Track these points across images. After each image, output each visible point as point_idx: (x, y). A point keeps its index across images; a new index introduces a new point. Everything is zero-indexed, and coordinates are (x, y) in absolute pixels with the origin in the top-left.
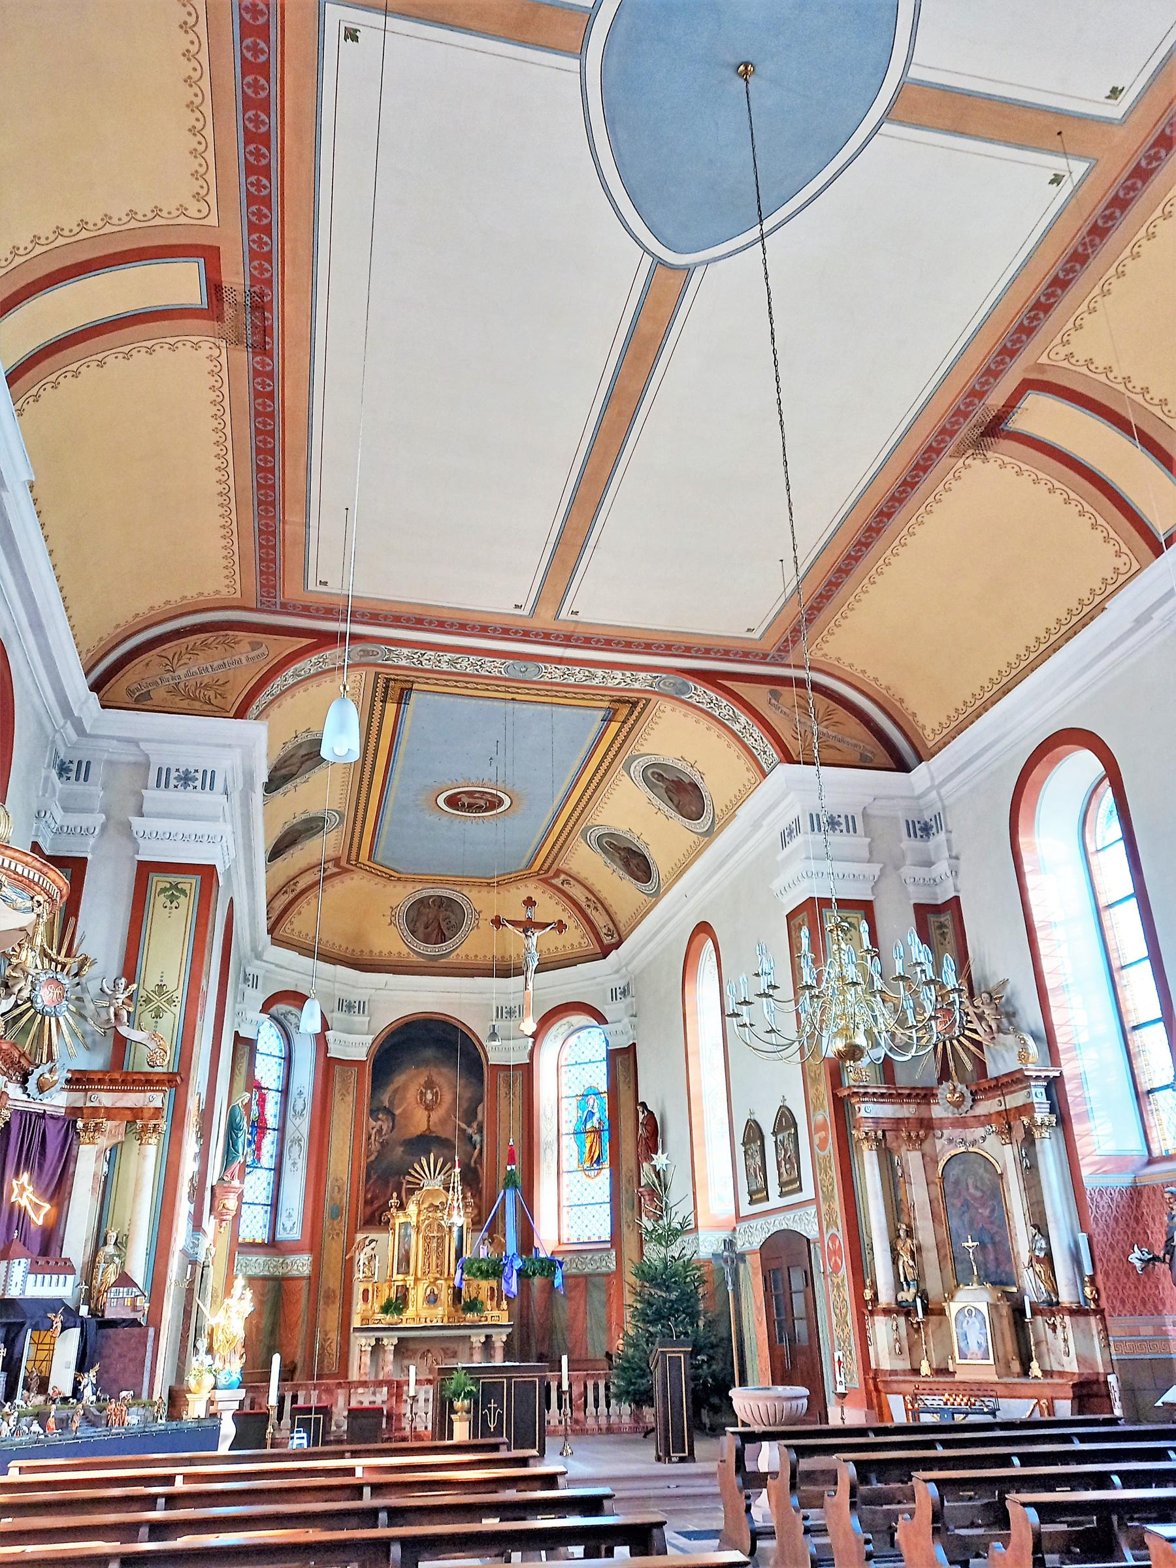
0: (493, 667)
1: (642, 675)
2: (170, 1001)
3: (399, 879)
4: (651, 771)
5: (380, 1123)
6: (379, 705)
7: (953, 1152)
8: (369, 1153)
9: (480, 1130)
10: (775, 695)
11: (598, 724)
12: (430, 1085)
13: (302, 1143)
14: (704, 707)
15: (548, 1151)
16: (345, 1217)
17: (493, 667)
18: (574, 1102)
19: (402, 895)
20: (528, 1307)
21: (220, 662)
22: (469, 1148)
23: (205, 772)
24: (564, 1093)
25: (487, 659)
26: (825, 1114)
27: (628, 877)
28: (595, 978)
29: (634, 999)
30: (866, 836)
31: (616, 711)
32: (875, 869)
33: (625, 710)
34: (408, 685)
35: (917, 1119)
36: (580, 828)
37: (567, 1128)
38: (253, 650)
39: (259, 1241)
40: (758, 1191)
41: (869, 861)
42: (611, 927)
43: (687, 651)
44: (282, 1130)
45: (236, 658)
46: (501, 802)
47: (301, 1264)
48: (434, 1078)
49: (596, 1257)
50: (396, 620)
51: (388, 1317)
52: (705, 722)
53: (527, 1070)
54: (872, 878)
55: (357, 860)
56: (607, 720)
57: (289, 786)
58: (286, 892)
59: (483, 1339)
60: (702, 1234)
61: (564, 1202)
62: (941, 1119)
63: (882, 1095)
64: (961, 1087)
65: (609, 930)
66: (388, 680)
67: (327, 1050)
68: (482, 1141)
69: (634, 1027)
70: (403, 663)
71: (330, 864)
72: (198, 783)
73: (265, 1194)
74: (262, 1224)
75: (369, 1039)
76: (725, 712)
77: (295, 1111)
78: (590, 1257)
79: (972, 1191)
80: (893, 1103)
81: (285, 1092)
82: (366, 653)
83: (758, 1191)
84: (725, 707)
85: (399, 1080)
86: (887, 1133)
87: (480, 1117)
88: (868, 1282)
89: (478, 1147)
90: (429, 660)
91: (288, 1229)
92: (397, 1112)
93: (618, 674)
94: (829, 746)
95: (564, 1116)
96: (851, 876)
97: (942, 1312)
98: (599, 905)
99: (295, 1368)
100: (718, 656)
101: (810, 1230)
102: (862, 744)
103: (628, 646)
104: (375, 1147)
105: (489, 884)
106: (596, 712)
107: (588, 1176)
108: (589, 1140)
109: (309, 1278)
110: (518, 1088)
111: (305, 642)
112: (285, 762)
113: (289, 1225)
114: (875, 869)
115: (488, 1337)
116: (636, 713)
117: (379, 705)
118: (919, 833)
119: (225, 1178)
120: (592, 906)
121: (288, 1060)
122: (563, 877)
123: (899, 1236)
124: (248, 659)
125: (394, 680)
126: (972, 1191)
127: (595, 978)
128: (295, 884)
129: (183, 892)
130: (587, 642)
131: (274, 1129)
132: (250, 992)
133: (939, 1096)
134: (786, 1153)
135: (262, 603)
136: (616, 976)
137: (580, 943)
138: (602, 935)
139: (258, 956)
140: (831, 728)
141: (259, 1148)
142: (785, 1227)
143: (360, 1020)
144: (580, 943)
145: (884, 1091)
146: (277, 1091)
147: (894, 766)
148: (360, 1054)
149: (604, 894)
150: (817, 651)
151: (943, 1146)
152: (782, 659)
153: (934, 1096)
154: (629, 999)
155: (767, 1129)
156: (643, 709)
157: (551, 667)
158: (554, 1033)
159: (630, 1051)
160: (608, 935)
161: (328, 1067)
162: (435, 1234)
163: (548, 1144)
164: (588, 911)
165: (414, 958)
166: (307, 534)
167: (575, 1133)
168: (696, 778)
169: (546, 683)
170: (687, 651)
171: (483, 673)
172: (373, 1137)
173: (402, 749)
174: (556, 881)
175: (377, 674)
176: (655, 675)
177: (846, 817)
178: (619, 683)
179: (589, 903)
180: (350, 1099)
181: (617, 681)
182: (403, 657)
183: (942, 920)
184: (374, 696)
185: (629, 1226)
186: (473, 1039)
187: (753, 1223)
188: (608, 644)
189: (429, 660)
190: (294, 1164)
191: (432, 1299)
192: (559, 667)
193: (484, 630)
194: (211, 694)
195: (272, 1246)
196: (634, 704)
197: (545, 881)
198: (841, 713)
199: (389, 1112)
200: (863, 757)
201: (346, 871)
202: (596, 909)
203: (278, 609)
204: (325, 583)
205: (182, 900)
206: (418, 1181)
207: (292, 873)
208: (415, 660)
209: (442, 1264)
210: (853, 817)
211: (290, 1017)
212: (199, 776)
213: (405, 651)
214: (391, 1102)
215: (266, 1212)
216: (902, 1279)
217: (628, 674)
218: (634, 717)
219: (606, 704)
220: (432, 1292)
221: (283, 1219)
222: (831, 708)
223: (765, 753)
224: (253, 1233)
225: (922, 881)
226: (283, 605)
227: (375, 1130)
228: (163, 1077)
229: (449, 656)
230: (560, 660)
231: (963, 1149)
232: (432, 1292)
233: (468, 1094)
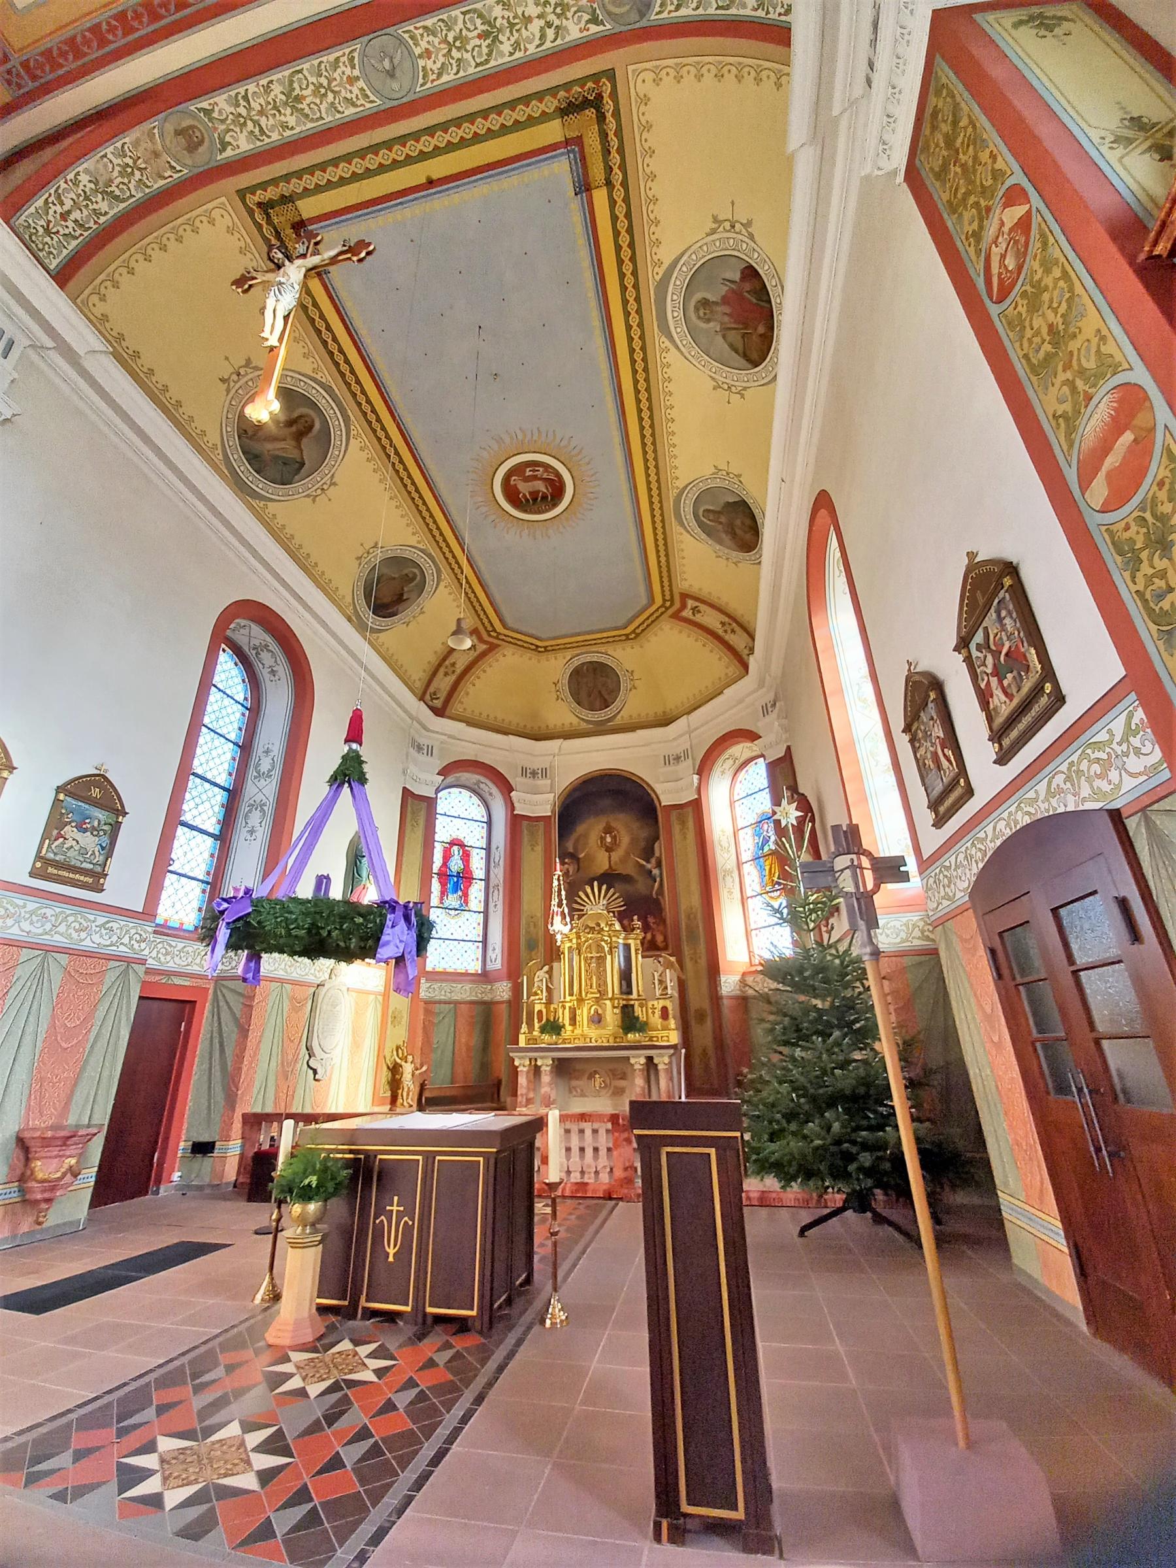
9: (659, 865)
12: (608, 830)
15: (728, 879)
16: (541, 948)
18: (749, 831)
19: (558, 667)
20: (720, 1026)
22: (650, 882)
24: (741, 824)
37: (746, 856)
44: (487, 880)
48: (613, 824)
51: (546, 1037)
53: (696, 807)
59: (643, 1061)
67: (513, 808)
69: (786, 729)
73: (475, 932)
81: (488, 849)
85: (581, 829)
87: (657, 854)
92: (581, 856)
99: (499, 1082)
109: (509, 1002)
110: (691, 824)
113: (493, 957)
115: (650, 1059)
121: (489, 823)
122: (690, 603)
136: (764, 689)
141: (466, 895)
143: (544, 783)
158: (720, 769)
159: (788, 756)
161: (516, 822)
162: (594, 954)
163: (730, 872)
165: (584, 725)
167: (756, 859)
174: (687, 613)
180: (539, 848)
187: (950, 860)
191: (597, 1020)
195: (485, 977)
197: (676, 616)
199: (574, 856)
202: (733, 631)
214: (575, 848)
220: (596, 1011)
221: (490, 953)
224: (465, 964)
233: (644, 834)
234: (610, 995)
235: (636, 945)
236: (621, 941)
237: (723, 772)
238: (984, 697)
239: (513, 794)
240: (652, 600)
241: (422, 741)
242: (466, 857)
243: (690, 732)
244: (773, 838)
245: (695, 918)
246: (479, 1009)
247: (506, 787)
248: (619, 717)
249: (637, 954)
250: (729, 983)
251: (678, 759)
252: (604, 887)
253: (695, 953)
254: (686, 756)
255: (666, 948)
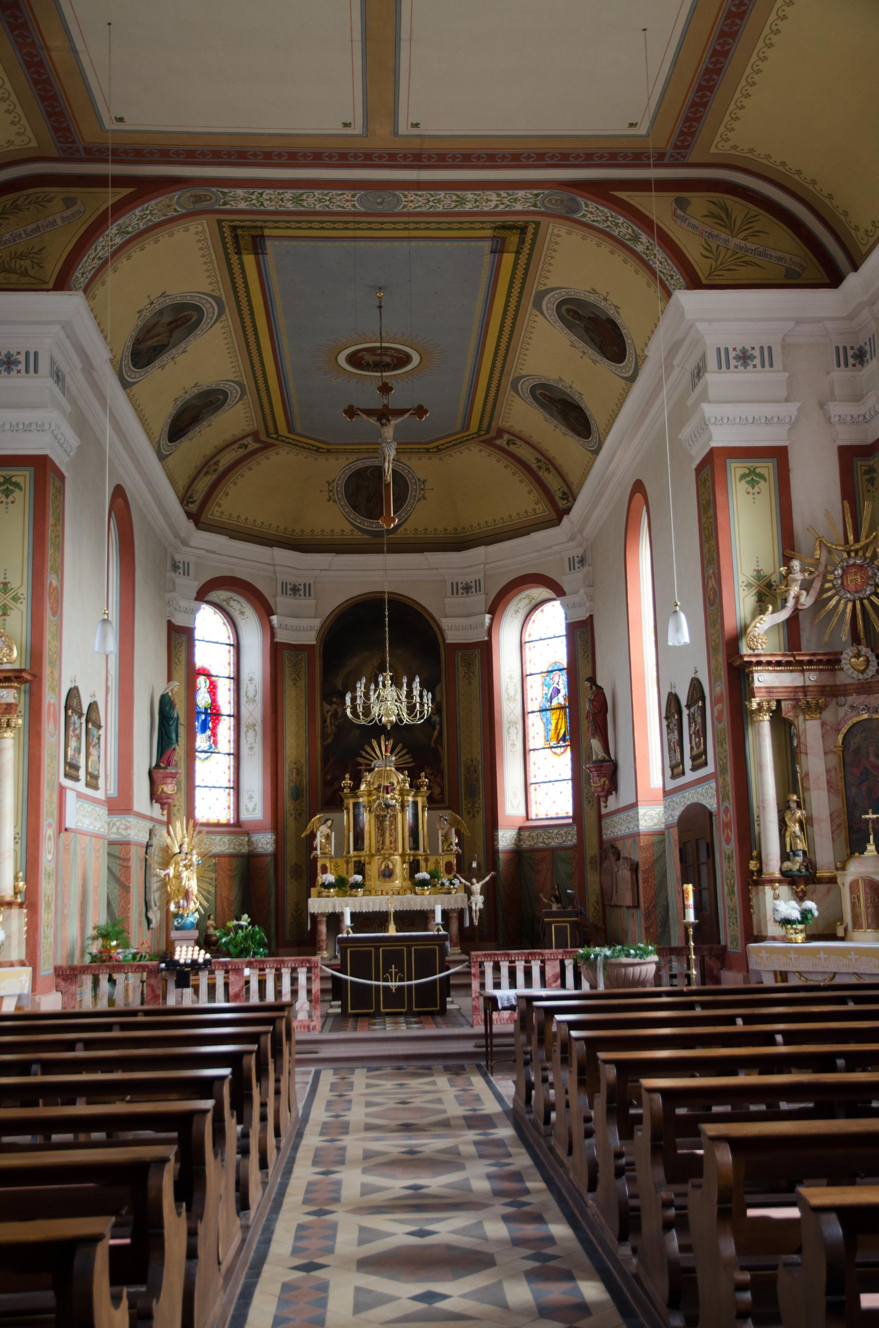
0: (346, 201)
1: (521, 194)
2: (15, 599)
3: (329, 451)
4: (564, 308)
5: (334, 706)
6: (234, 258)
7: (855, 720)
8: (324, 736)
10: (682, 204)
11: (488, 259)
13: (257, 728)
14: (601, 226)
15: (513, 730)
17: (346, 201)
21: (33, 226)
23: (27, 354)
24: (529, 670)
25: (334, 192)
26: (721, 688)
27: (571, 433)
28: (551, 547)
29: (590, 568)
30: (785, 369)
31: (504, 240)
32: (791, 409)
33: (513, 239)
34: (259, 233)
35: (818, 686)
36: (507, 381)
38: (68, 208)
39: (223, 821)
40: (677, 766)
41: (787, 400)
42: (567, 491)
43: (563, 160)
44: (237, 716)
45: (50, 219)
46: (407, 359)
47: (265, 842)
49: (534, 834)
50: (217, 157)
52: (606, 247)
54: (787, 420)
55: (277, 432)
56: (498, 250)
57: (165, 358)
58: (207, 473)
60: (642, 810)
61: (532, 780)
62: (845, 685)
63: (779, 663)
64: (864, 650)
65: (564, 493)
66: (234, 228)
67: (273, 635)
68: (441, 722)
69: (591, 598)
70: (243, 206)
71: (249, 439)
72: (22, 367)
74: (226, 806)
75: (317, 623)
76: (624, 230)
77: (247, 697)
78: (556, 831)
79: (872, 759)
80: (792, 671)
81: (237, 679)
82: (198, 199)
83: (677, 766)
84: (624, 227)
86: (783, 703)
88: (755, 853)
89: (438, 727)
90: (270, 199)
91: (251, 809)
93: (492, 195)
94: (747, 263)
95: (530, 694)
96: (725, 420)
97: (832, 880)
98: (550, 466)
100: (603, 161)
101: (711, 803)
102: (788, 256)
103: (491, 160)
104: (331, 730)
105: (428, 450)
106: (481, 244)
107: (556, 754)
108: (555, 717)
110: (477, 669)
111: (125, 192)
112: (148, 332)
113: (251, 806)
114: (791, 409)
116: (528, 240)
117: (234, 258)
118: (851, 361)
119: (162, 765)
120: (544, 468)
121: (237, 647)
122: (506, 437)
123: (789, 808)
124: (63, 219)
125: (242, 227)
126: (872, 759)
127: (551, 547)
128: (216, 464)
129: (17, 485)
130: (441, 160)
131: (229, 716)
132: (180, 580)
133: (843, 661)
134: (696, 726)
135: (64, 151)
136: (574, 543)
137: (534, 510)
138: (558, 500)
139: (185, 543)
140: (751, 239)
141: (214, 735)
142: (695, 800)
144: (534, 510)
145: (779, 658)
146: (229, 678)
147: (827, 281)
148: (310, 639)
149: (552, 453)
150: (723, 143)
151: (846, 714)
152: (684, 157)
153: (839, 661)
154: (585, 569)
155: (684, 702)
156: (535, 234)
157: (411, 195)
160: (563, 499)
163: (512, 723)
164: (540, 474)
165: (358, 535)
166: (78, 61)
168: (612, 313)
169: (409, 214)
170: (588, 159)
171: (335, 209)
172: (328, 720)
173: (279, 304)
174: (502, 442)
175: (219, 222)
176: (535, 192)
177: (762, 348)
178: (497, 206)
179: (539, 464)
181: (493, 204)
182: (240, 199)
183: (871, 463)
184: (225, 249)
185: (589, 802)
186: (425, 615)
188: (466, 160)
189: (270, 200)
190: (251, 748)
192: (420, 193)
193: (317, 158)
194: (26, 263)
195: (237, 827)
196: (523, 229)
198: (765, 220)
200: (789, 273)
201: (266, 447)
202: (547, 469)
203: (83, 155)
204: (121, 120)
205: (17, 494)
206: (368, 762)
207: (209, 451)
208: (254, 202)
209: (396, 841)
210: (770, 348)
211: (232, 603)
212: (22, 358)
213: (240, 192)
215: (229, 794)
216: (788, 850)
217: (503, 194)
218: (527, 245)
219: (489, 233)
222: (752, 213)
223: (672, 276)
225: (849, 418)
226: (88, 150)
227: (330, 714)
228: (8, 674)
229: (289, 194)
230: (418, 185)
231: (866, 716)
232: (387, 867)
234: (400, 851)
235: (423, 802)
236: (410, 799)
237: (517, 612)
238: (692, 749)
239: (274, 619)
240: (468, 428)
241: (178, 557)
242: (213, 690)
243: (485, 564)
244: (564, 691)
245: (475, 771)
246: (236, 862)
247: (265, 609)
248: (401, 529)
249: (423, 811)
250: (505, 838)
251: (467, 588)
252: (404, 752)
253: (473, 807)
254: (478, 589)
255: (442, 801)
